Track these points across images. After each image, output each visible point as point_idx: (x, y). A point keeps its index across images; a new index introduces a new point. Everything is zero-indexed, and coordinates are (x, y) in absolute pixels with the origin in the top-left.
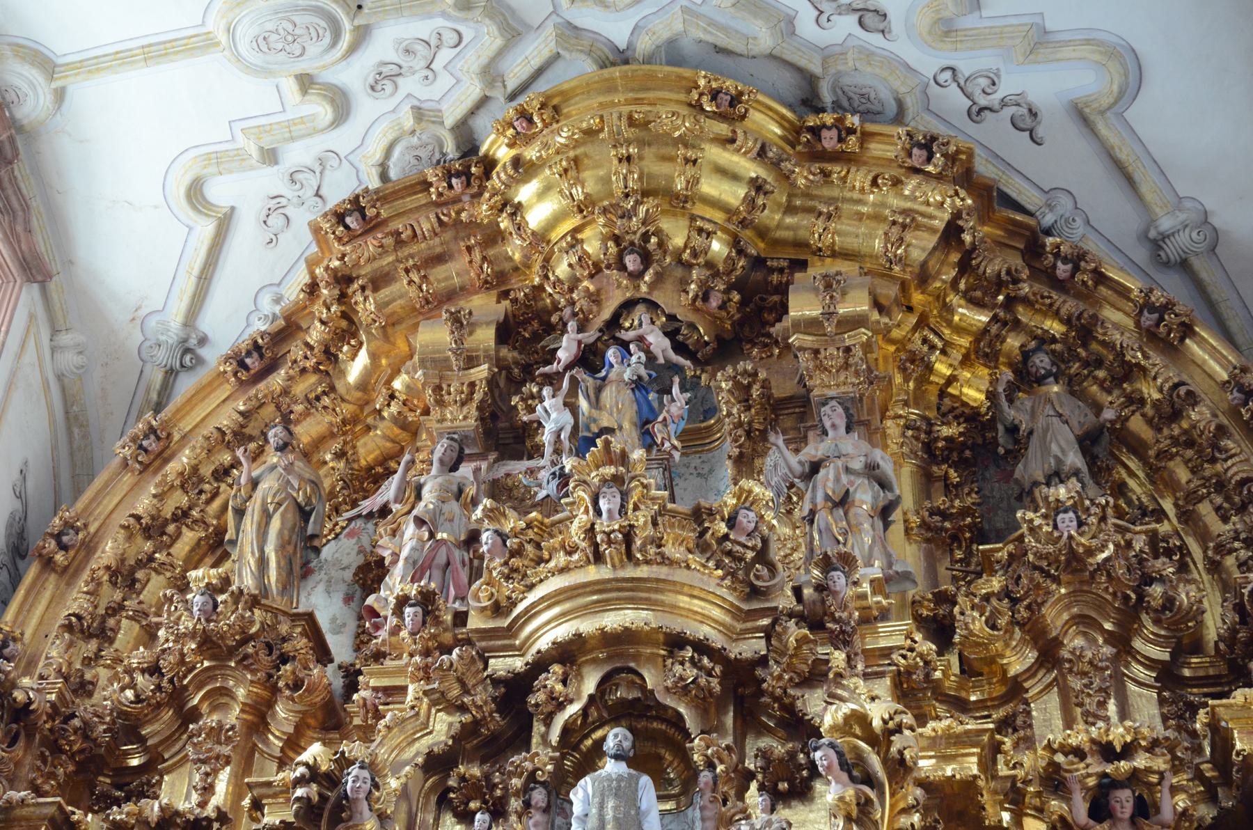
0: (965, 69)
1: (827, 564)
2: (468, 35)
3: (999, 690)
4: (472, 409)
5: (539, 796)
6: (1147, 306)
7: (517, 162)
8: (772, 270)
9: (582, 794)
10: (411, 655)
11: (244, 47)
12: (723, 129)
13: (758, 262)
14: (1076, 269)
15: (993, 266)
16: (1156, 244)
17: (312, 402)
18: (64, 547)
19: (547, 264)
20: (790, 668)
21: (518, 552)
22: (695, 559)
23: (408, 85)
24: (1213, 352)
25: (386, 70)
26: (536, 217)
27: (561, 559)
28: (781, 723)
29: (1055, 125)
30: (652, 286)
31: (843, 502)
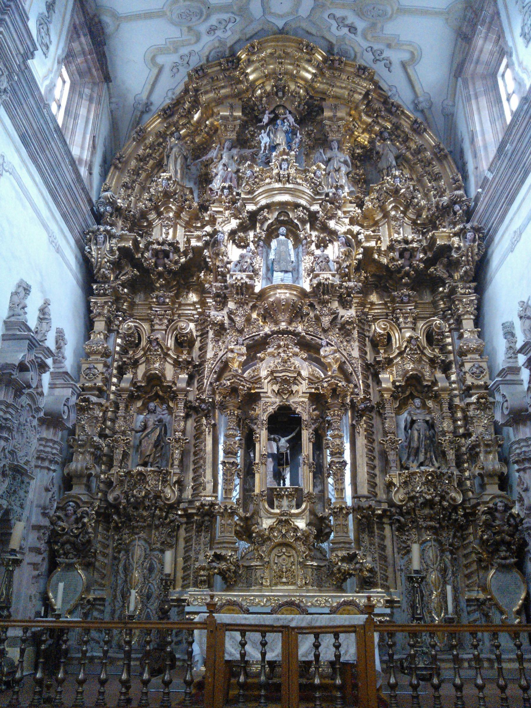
0: (376, 47)
1: (337, 188)
2: (238, 19)
3: (371, 223)
5: (261, 243)
6: (416, 121)
8: (315, 100)
9: (274, 244)
11: (174, 17)
12: (308, 57)
13: (311, 97)
14: (397, 109)
15: (377, 106)
16: (416, 105)
17: (184, 125)
18: (120, 162)
19: (254, 91)
20: (326, 215)
21: (256, 177)
23: (219, 33)
24: (431, 137)
25: (213, 28)
26: (251, 77)
27: (268, 180)
28: (321, 228)
29: (397, 68)
31: (338, 170)
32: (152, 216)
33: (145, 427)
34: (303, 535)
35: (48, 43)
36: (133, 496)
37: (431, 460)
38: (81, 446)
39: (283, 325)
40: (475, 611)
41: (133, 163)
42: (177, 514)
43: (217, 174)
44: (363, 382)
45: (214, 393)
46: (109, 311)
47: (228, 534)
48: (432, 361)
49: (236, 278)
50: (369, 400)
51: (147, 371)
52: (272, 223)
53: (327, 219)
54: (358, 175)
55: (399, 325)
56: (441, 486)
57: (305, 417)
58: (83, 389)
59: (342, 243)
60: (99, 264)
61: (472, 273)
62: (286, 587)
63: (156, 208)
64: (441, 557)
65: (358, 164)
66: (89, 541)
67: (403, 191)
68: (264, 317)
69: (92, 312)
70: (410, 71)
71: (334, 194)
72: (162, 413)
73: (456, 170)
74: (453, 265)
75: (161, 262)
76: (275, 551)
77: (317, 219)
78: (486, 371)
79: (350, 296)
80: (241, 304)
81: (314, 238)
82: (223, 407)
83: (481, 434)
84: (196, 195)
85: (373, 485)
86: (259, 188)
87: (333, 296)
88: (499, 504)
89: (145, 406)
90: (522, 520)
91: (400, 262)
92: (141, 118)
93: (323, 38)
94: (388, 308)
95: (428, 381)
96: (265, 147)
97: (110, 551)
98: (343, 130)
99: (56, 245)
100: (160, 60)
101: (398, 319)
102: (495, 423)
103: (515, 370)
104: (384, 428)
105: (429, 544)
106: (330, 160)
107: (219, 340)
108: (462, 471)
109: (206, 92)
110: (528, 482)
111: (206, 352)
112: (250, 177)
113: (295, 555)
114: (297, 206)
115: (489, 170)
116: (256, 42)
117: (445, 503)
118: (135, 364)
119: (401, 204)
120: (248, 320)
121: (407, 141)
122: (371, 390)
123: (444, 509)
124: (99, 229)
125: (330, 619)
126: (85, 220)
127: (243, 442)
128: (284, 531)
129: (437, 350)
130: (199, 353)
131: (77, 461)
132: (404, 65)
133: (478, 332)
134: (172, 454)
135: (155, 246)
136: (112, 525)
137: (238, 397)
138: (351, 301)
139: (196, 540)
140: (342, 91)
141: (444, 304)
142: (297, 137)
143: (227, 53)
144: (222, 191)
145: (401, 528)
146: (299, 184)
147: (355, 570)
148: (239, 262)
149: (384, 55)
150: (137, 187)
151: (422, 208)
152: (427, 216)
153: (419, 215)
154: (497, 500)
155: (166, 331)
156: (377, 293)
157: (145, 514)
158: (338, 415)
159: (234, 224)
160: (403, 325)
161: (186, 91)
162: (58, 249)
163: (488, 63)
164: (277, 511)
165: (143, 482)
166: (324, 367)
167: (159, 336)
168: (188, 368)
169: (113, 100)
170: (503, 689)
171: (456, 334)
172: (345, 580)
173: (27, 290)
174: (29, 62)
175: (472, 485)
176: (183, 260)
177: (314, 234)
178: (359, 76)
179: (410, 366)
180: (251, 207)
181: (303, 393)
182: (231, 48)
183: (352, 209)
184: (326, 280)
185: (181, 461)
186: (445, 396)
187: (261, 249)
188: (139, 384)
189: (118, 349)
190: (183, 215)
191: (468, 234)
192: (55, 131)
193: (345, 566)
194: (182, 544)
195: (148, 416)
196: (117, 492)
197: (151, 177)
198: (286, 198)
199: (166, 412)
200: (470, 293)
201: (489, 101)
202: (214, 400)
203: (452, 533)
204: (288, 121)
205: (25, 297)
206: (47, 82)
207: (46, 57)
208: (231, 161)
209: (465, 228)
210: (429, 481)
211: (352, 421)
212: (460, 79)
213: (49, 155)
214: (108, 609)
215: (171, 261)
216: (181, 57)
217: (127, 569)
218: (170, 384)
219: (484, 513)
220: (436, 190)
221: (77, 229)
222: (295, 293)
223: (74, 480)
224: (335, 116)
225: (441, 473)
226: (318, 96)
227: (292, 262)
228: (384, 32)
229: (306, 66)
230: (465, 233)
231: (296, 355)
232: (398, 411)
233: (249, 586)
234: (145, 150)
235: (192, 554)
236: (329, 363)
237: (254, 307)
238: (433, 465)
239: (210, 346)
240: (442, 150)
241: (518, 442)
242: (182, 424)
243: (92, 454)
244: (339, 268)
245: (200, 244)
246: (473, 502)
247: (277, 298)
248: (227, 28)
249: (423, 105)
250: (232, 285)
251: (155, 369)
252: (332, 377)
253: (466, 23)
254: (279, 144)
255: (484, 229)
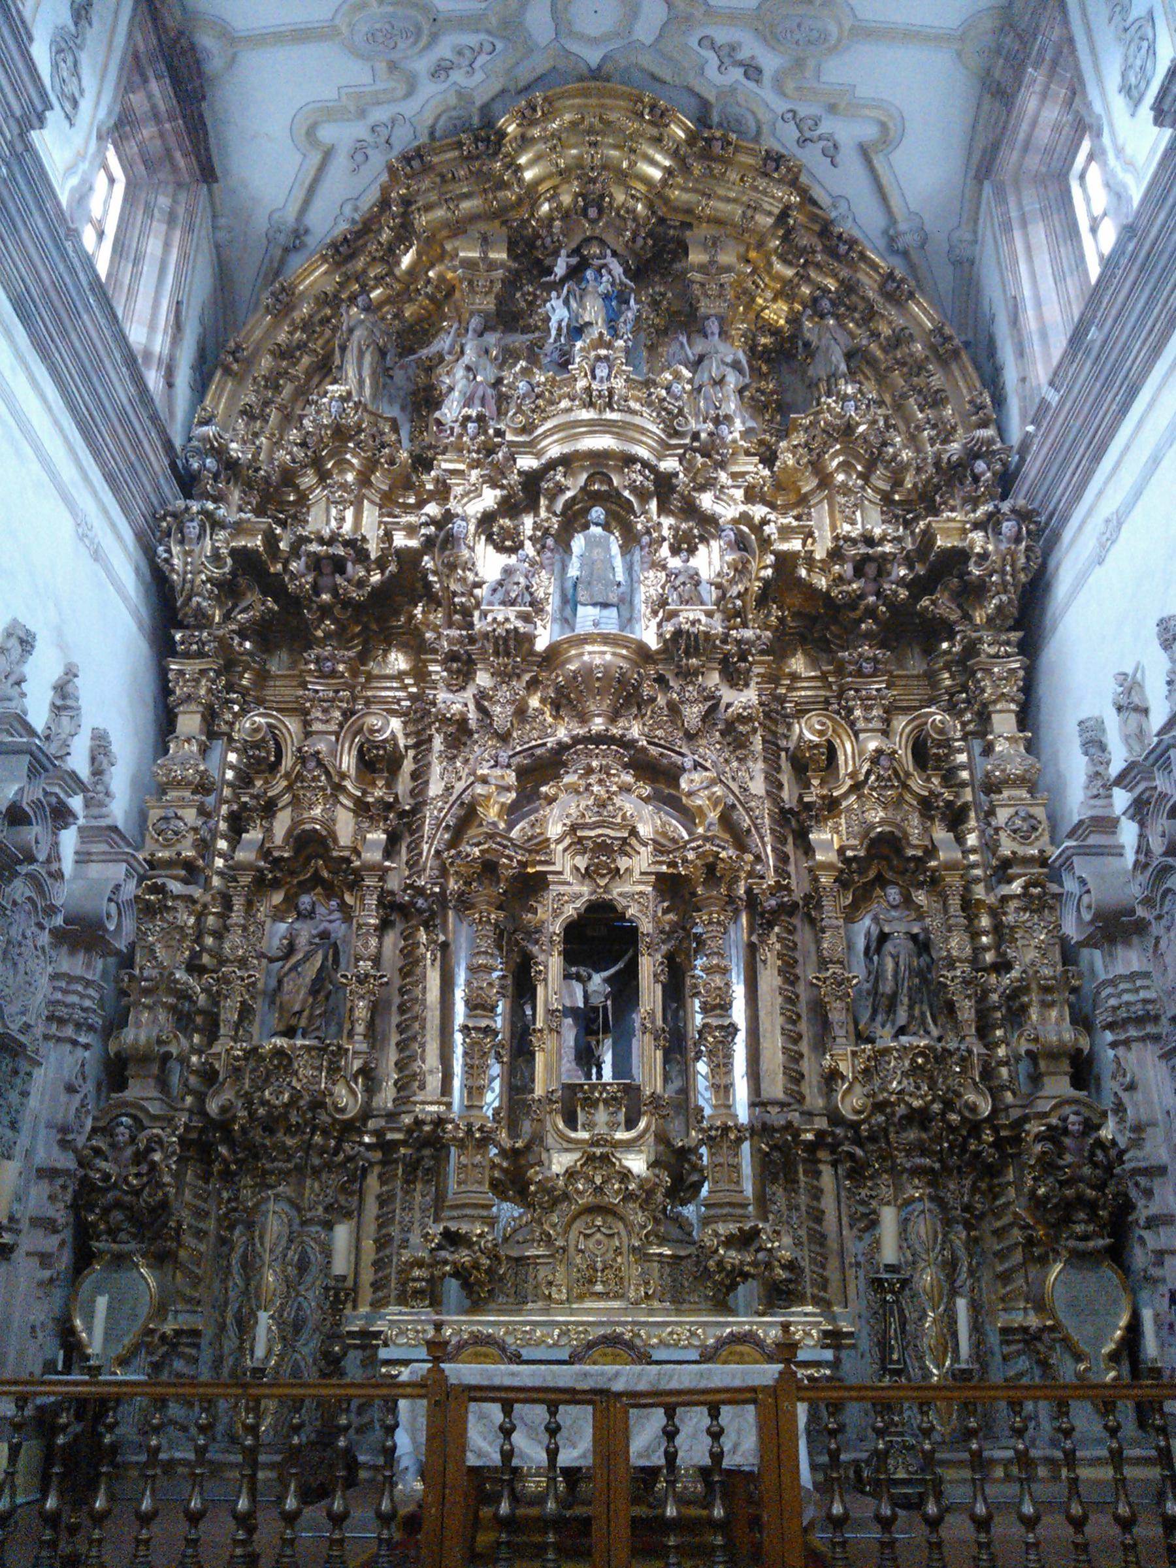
0: (803, 111)
1: (717, 421)
2: (500, 46)
3: (793, 498)
4: (491, 299)
5: (550, 542)
6: (891, 276)
7: (523, 137)
8: (670, 227)
9: (578, 543)
10: (469, 452)
12: (655, 132)
13: (662, 221)
14: (850, 249)
16: (892, 240)
17: (379, 279)
18: (236, 360)
19: (534, 205)
20: (693, 480)
21: (538, 396)
22: (646, 411)
23: (457, 76)
24: (924, 310)
25: (443, 64)
26: (529, 175)
27: (564, 404)
30: (603, 228)
31: (720, 382)
32: (308, 479)
33: (291, 949)
34: (641, 1187)
35: (77, 95)
36: (264, 1103)
37: (923, 1023)
38: (146, 992)
39: (598, 724)
40: (1019, 1353)
41: (266, 363)
42: (361, 1144)
43: (451, 389)
44: (774, 849)
45: (444, 872)
46: (210, 690)
47: (474, 1188)
48: (926, 805)
49: (495, 619)
50: (787, 888)
51: (295, 824)
52: (574, 498)
53: (694, 489)
54: (763, 393)
55: (852, 724)
56: (945, 1078)
57: (646, 926)
58: (152, 864)
59: (729, 544)
60: (188, 586)
61: (1014, 611)
62: (602, 1304)
63: (317, 463)
64: (945, 1235)
65: (764, 368)
66: (164, 1205)
67: (862, 428)
68: (556, 706)
69: (171, 692)
70: (879, 162)
71: (711, 434)
72: (328, 918)
73: (978, 385)
74: (974, 592)
75: (325, 581)
76: (578, 1225)
77: (672, 489)
78: (1045, 824)
79: (745, 660)
80: (504, 676)
81: (666, 532)
82: (464, 903)
83: (1033, 964)
84: (404, 434)
85: (795, 1077)
86: (545, 419)
87: (710, 660)
88: (1072, 1118)
89: (290, 902)
90: (1122, 1153)
91: (855, 586)
92: (282, 262)
93: (690, 91)
94: (830, 685)
95: (916, 847)
96: (559, 329)
97: (211, 1225)
98: (730, 294)
99: (92, 543)
100: (328, 133)
101: (850, 711)
102: (1064, 941)
103: (1107, 824)
104: (819, 949)
105: (919, 1206)
106: (701, 359)
107: (455, 757)
108: (991, 1046)
109: (428, 208)
110: (1136, 1070)
111: (427, 782)
112: (524, 397)
113: (623, 1233)
114: (629, 460)
115: (1051, 384)
116: (539, 96)
117: (954, 1117)
118: (269, 809)
119: (858, 457)
120: (521, 712)
121: (871, 319)
122: (791, 868)
123: (952, 1129)
124: (187, 509)
125: (701, 1374)
126: (157, 488)
127: (509, 982)
128: (598, 1180)
129: (936, 781)
130: (411, 785)
131: (138, 1025)
132: (865, 152)
133: (1027, 740)
134: (351, 1010)
135: (314, 547)
136: (217, 1167)
137: (498, 882)
138: (749, 670)
139: (404, 1201)
140: (729, 207)
141: (952, 677)
142: (629, 308)
143: (476, 121)
144: (463, 425)
145: (857, 1172)
146: (633, 412)
147: (755, 1264)
148: (500, 584)
149: (823, 129)
150: (274, 416)
151: (904, 467)
152: (915, 485)
153: (897, 483)
154: (1067, 1110)
155: (337, 734)
156: (806, 653)
157: (290, 1142)
158: (719, 923)
159: (490, 498)
160: (861, 724)
161: (384, 203)
162: (96, 551)
163: (1048, 151)
164: (583, 1135)
165: (286, 1072)
166: (689, 816)
167: (322, 747)
168: (386, 819)
169: (222, 221)
170: (1078, 1524)
171: (977, 745)
172: (733, 1287)
173: (26, 643)
174: (34, 135)
175: (1013, 1077)
176: (376, 578)
177: (667, 522)
178: (766, 175)
179: (876, 815)
180: (527, 463)
181: (642, 874)
182: (485, 109)
183: (751, 468)
184: (693, 623)
185: (371, 1025)
186: (953, 880)
187: (549, 554)
188: (276, 854)
189: (230, 775)
190: (377, 477)
191: (1005, 524)
192: (92, 289)
193: (733, 1256)
194: (371, 1208)
195: (297, 926)
196: (227, 1095)
197: (303, 394)
198: (603, 442)
199: (337, 915)
200: (1008, 655)
201: (1050, 234)
202: (443, 888)
203: (968, 1183)
204: (610, 272)
205: (22, 660)
206: (74, 181)
207: (71, 125)
208: (484, 361)
209: (998, 510)
210: (919, 1067)
211: (750, 933)
212: (987, 185)
213: (77, 344)
214: (207, 1355)
215: (349, 581)
216: (373, 130)
217: (250, 1266)
218: (346, 854)
219: (1039, 1138)
220: (934, 427)
221: (140, 508)
222: (624, 652)
223: (131, 1070)
224: (712, 262)
225: (944, 1050)
226: (675, 219)
227: (619, 584)
228: (823, 79)
229: (651, 152)
230: (999, 523)
231: (625, 789)
232: (851, 914)
233: (520, 1301)
234: (291, 333)
235: (394, 1231)
236: (700, 807)
237: (533, 685)
238: (928, 1032)
239: (436, 769)
240: (948, 339)
241: (1112, 982)
242: (373, 942)
243: (172, 1009)
244: (723, 597)
245: (414, 543)
246: (1015, 1113)
247: (584, 663)
248: (477, 65)
249: (909, 240)
250: (486, 636)
251: (314, 820)
252: (706, 839)
253: (1001, 61)
254: (589, 324)
255: (1039, 514)
